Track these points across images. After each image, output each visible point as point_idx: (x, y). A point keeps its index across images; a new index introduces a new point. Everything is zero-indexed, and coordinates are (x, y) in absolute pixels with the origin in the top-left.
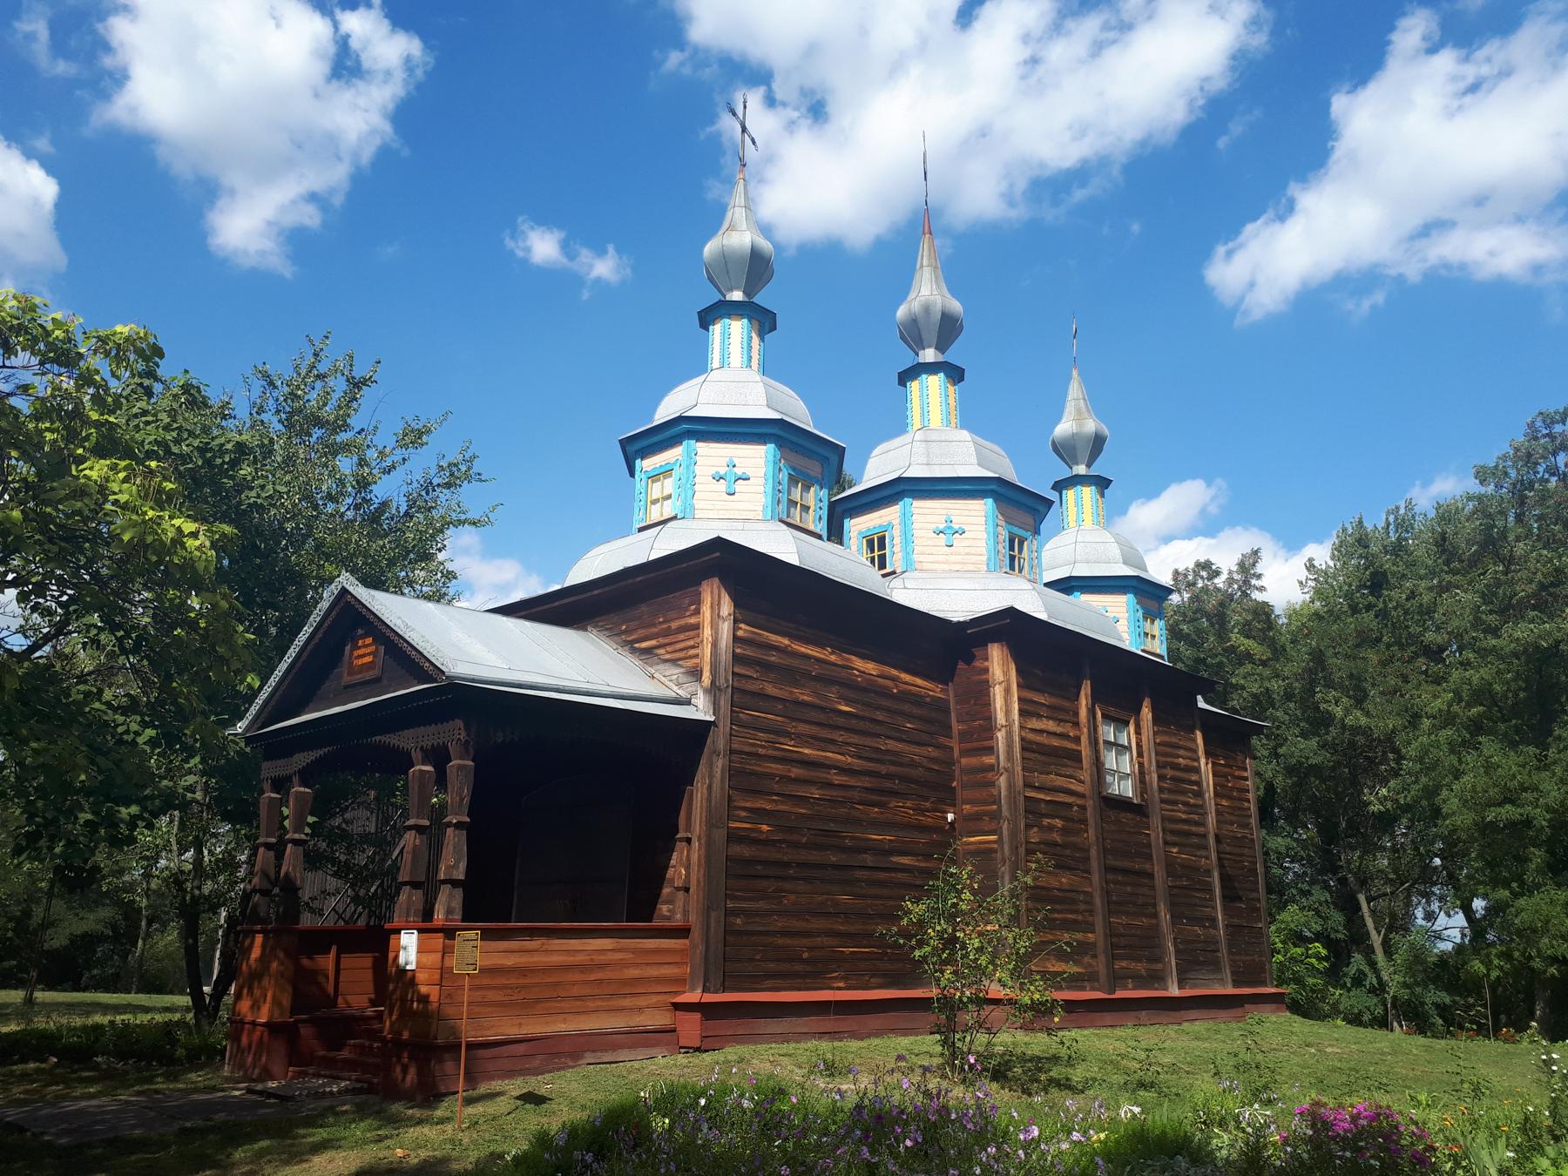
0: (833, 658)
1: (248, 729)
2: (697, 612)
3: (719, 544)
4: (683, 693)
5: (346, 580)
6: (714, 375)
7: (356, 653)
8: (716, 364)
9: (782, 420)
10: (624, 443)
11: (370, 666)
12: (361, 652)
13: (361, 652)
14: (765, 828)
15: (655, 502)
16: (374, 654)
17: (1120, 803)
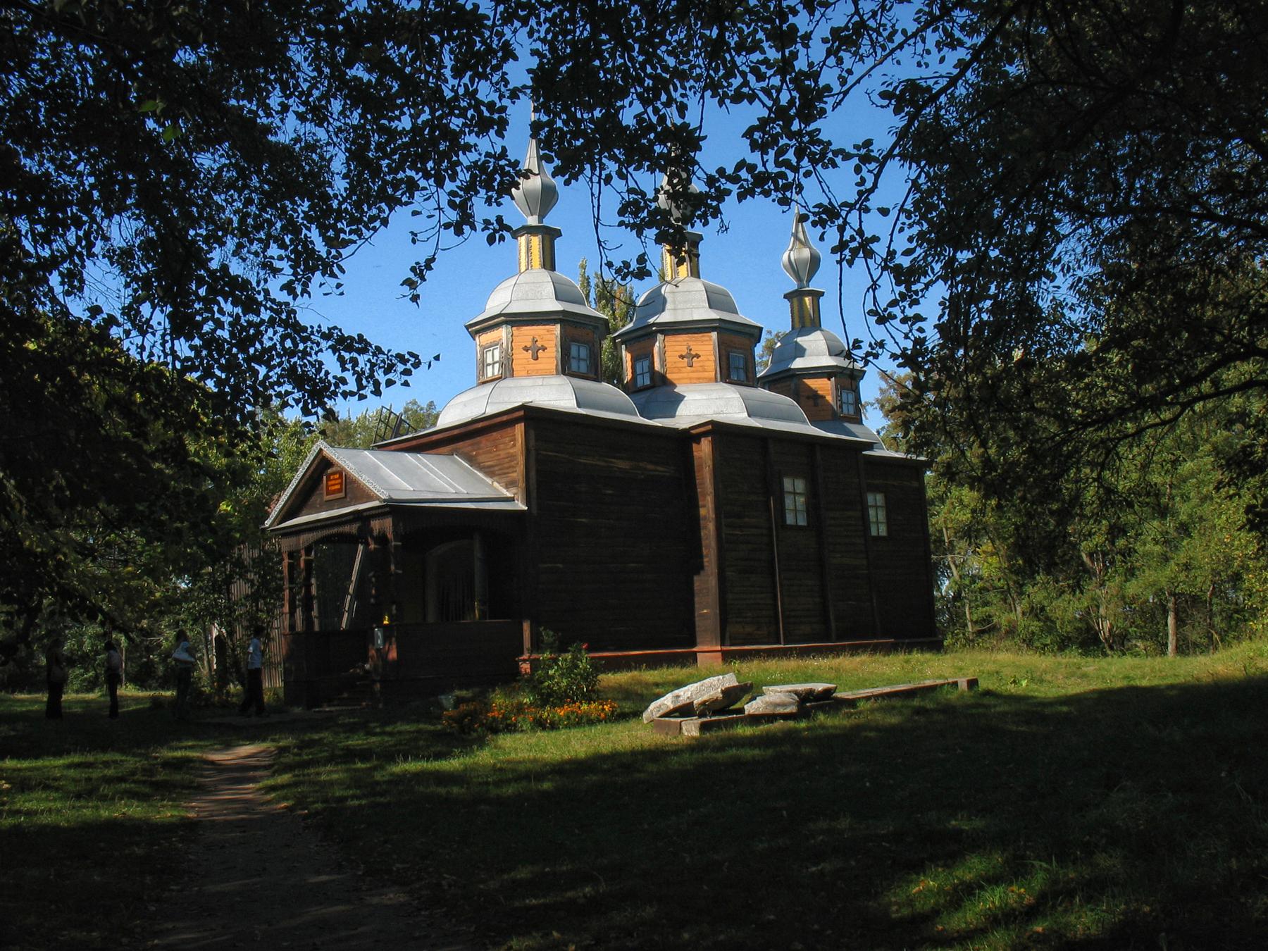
0: (598, 463)
1: (271, 525)
2: (514, 445)
3: (523, 407)
4: (509, 495)
5: (321, 444)
6: (522, 278)
7: (330, 483)
8: (523, 268)
9: (564, 312)
10: (467, 327)
11: (339, 491)
12: (333, 482)
13: (333, 482)
14: (561, 566)
15: (489, 365)
16: (341, 484)
17: (797, 528)
